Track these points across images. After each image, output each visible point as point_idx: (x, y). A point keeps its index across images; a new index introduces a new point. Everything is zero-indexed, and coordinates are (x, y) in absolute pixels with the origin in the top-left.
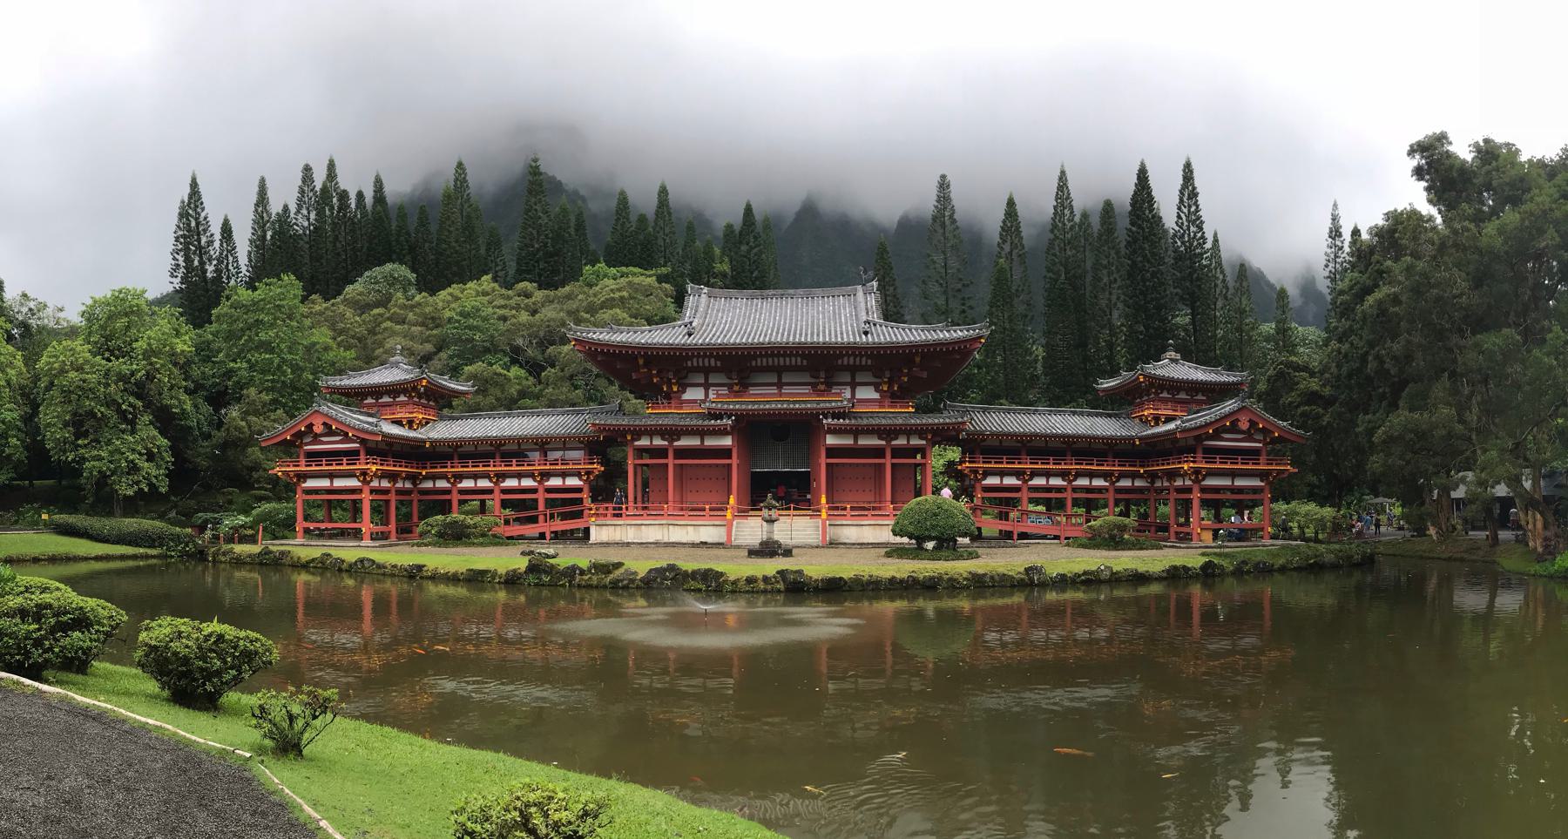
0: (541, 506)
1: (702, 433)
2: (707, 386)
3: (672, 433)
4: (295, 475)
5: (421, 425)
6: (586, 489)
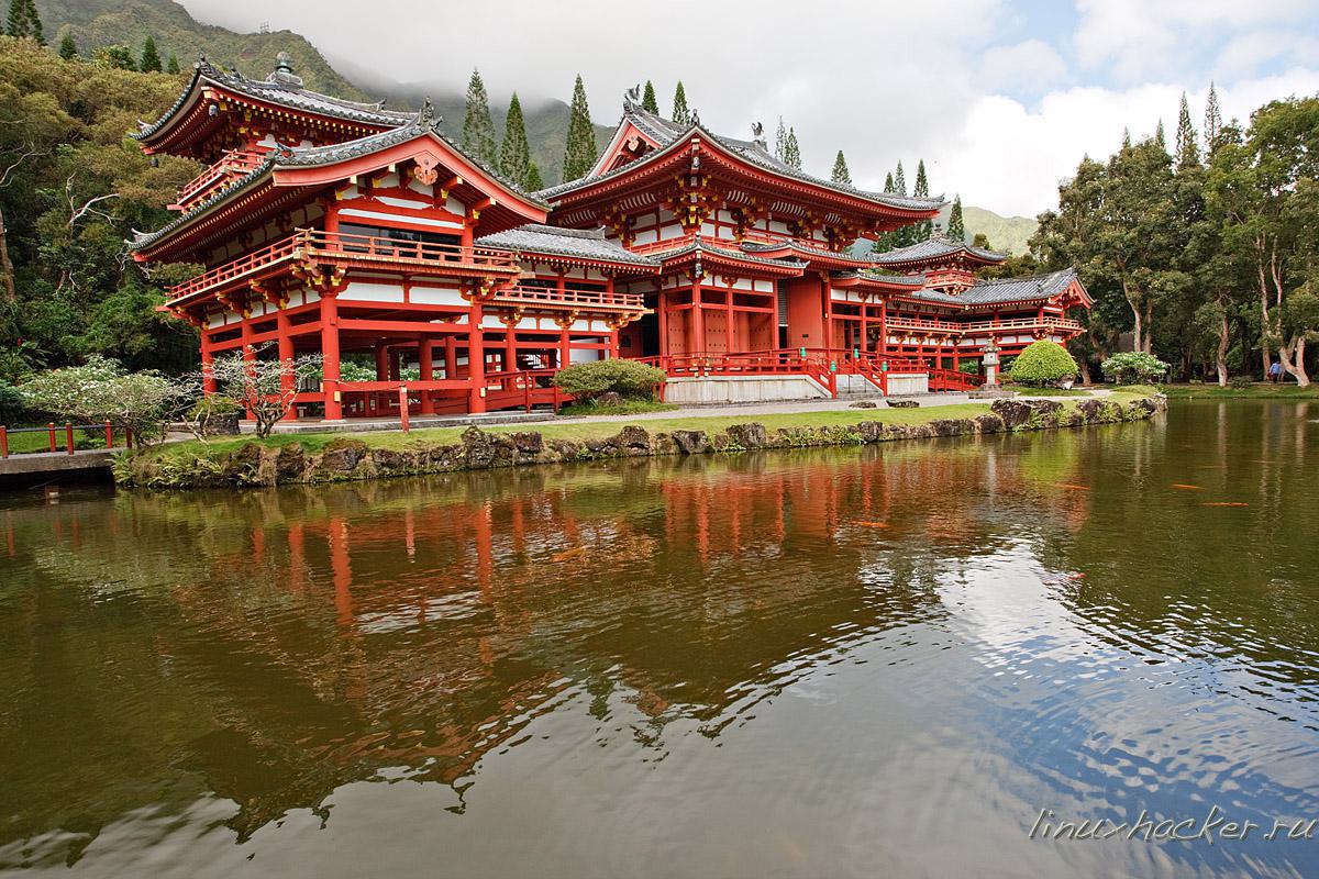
1: (755, 274)
2: (718, 224)
3: (731, 272)
6: (615, 338)
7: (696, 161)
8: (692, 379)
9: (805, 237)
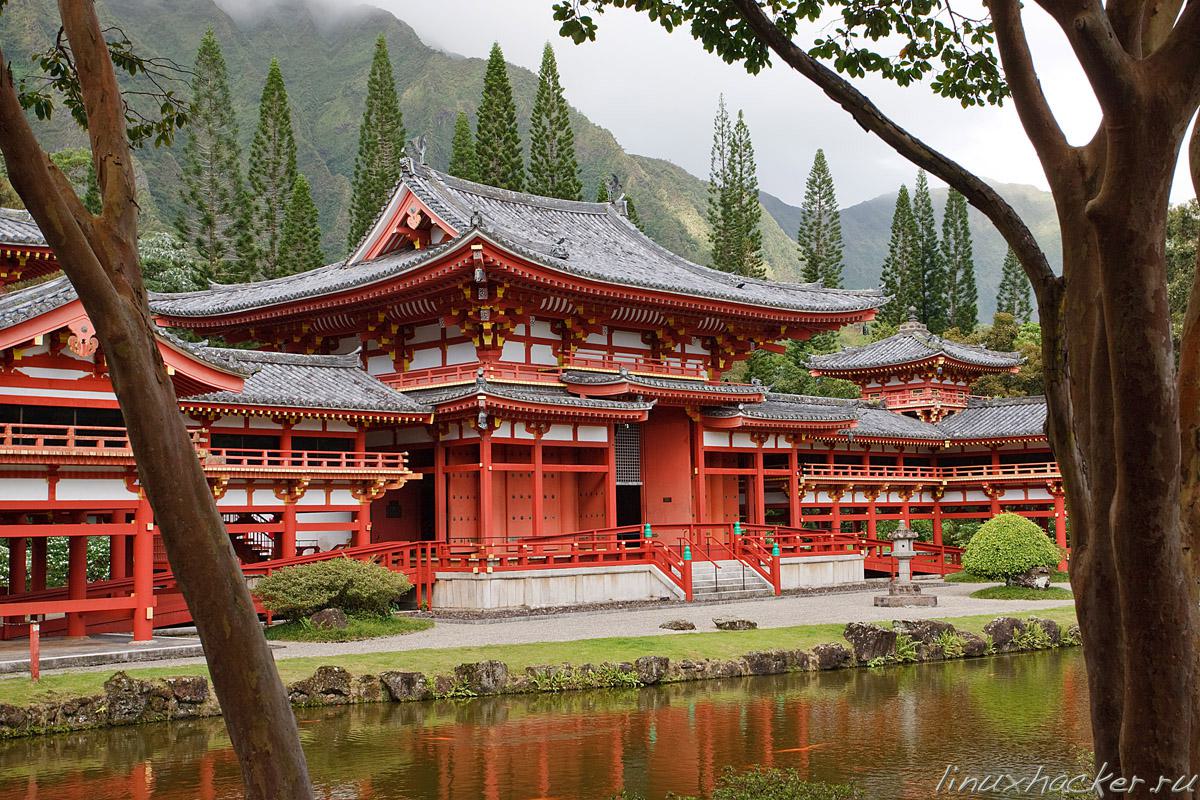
1: (576, 421)
2: (529, 341)
3: (540, 420)
6: (366, 515)
7: (478, 274)
8: (471, 575)
9: (670, 354)
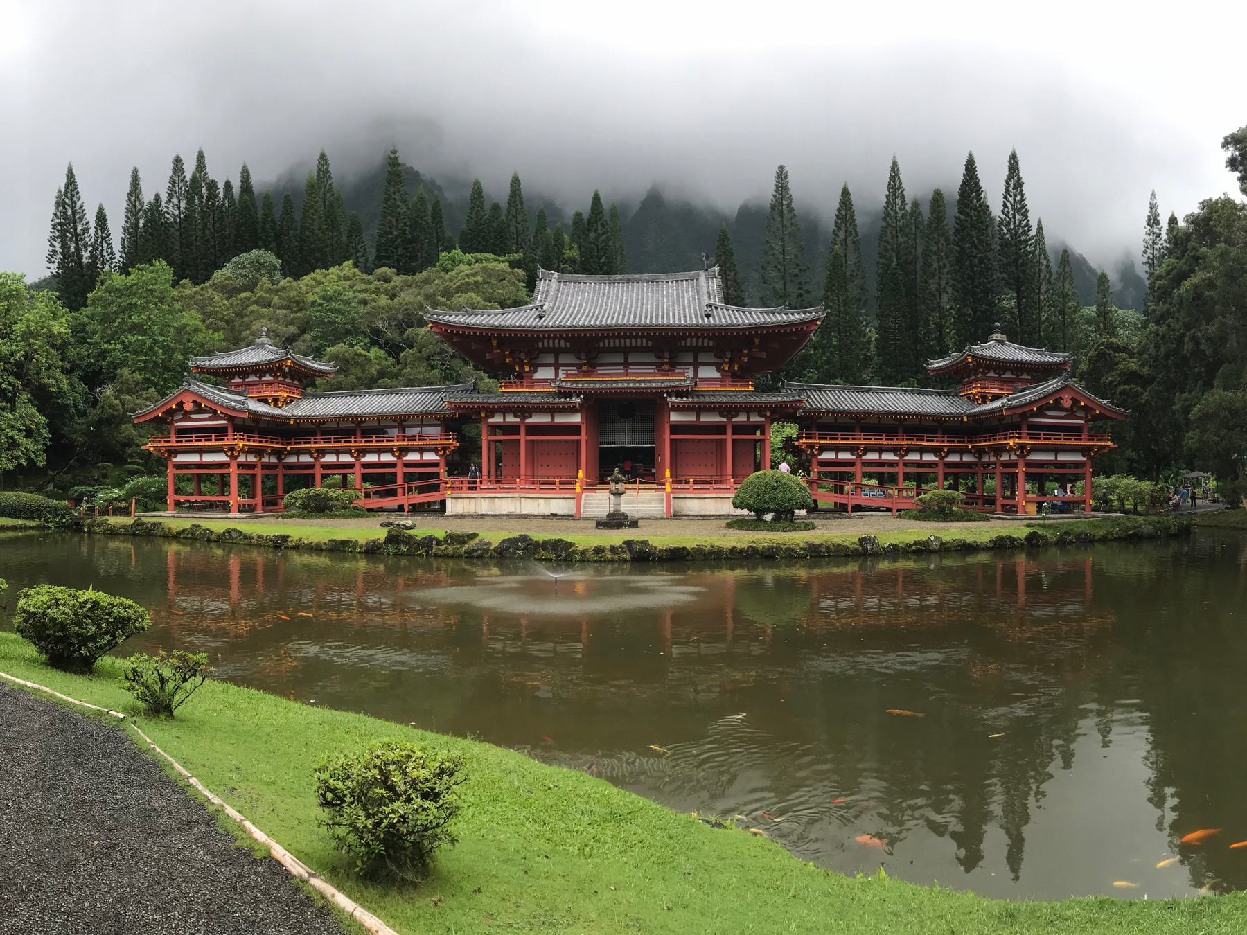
0: (400, 480)
1: (552, 410)
2: (557, 366)
3: (524, 411)
4: (166, 451)
5: (286, 403)
